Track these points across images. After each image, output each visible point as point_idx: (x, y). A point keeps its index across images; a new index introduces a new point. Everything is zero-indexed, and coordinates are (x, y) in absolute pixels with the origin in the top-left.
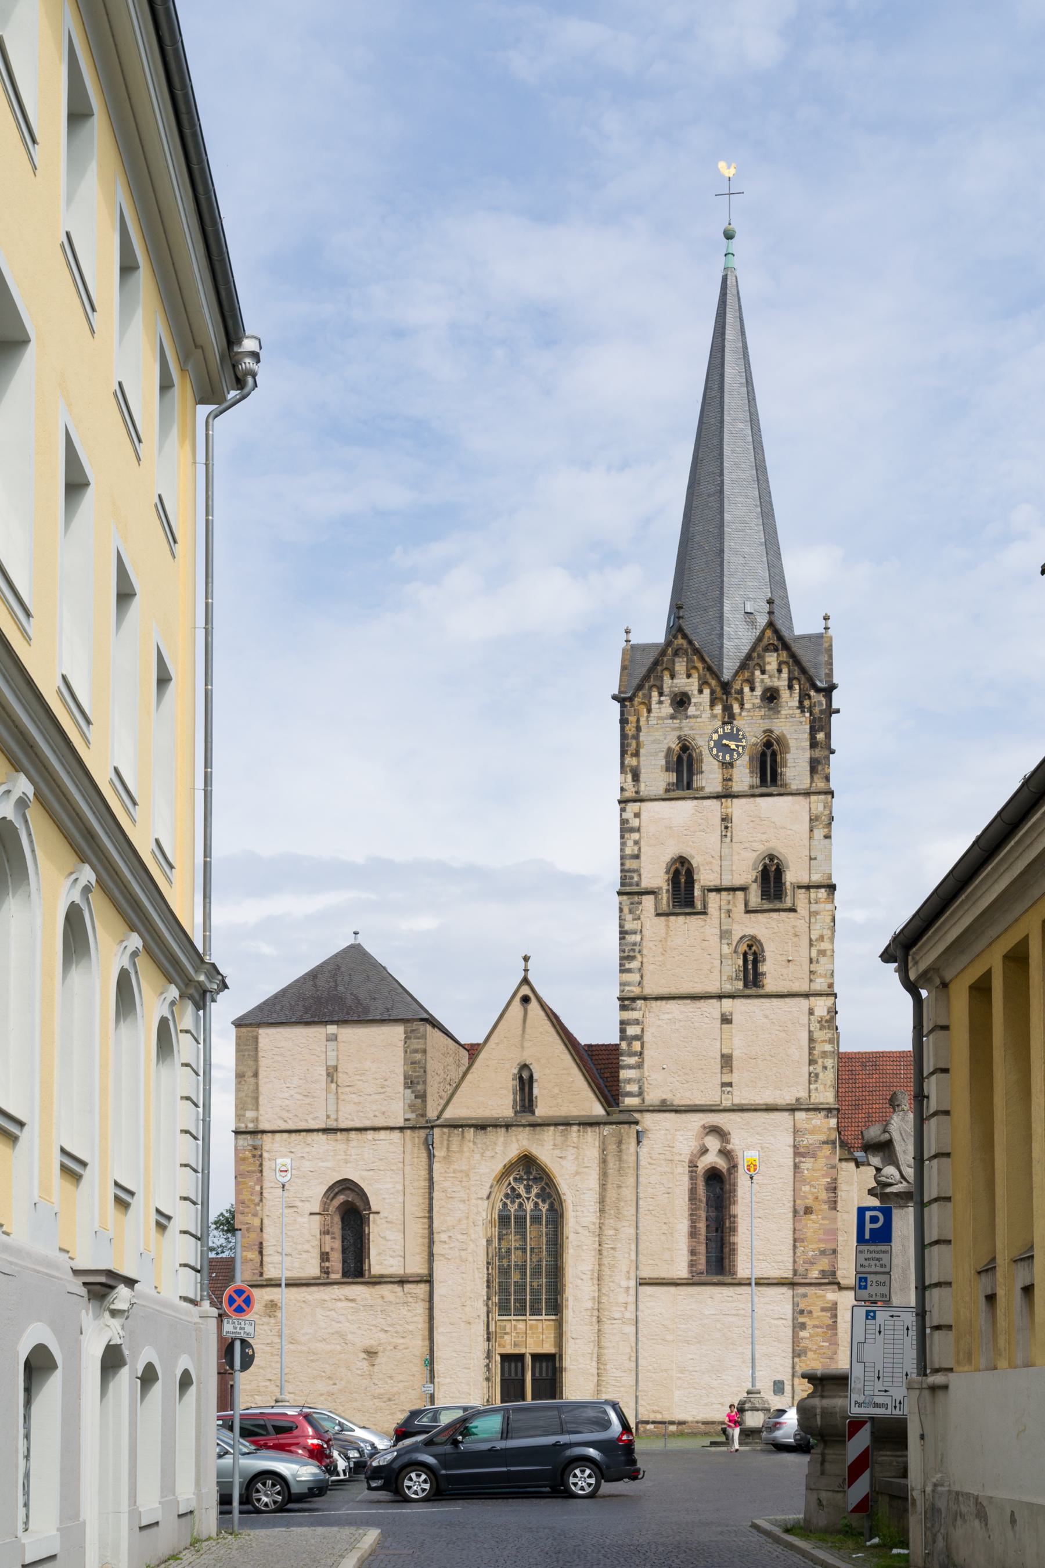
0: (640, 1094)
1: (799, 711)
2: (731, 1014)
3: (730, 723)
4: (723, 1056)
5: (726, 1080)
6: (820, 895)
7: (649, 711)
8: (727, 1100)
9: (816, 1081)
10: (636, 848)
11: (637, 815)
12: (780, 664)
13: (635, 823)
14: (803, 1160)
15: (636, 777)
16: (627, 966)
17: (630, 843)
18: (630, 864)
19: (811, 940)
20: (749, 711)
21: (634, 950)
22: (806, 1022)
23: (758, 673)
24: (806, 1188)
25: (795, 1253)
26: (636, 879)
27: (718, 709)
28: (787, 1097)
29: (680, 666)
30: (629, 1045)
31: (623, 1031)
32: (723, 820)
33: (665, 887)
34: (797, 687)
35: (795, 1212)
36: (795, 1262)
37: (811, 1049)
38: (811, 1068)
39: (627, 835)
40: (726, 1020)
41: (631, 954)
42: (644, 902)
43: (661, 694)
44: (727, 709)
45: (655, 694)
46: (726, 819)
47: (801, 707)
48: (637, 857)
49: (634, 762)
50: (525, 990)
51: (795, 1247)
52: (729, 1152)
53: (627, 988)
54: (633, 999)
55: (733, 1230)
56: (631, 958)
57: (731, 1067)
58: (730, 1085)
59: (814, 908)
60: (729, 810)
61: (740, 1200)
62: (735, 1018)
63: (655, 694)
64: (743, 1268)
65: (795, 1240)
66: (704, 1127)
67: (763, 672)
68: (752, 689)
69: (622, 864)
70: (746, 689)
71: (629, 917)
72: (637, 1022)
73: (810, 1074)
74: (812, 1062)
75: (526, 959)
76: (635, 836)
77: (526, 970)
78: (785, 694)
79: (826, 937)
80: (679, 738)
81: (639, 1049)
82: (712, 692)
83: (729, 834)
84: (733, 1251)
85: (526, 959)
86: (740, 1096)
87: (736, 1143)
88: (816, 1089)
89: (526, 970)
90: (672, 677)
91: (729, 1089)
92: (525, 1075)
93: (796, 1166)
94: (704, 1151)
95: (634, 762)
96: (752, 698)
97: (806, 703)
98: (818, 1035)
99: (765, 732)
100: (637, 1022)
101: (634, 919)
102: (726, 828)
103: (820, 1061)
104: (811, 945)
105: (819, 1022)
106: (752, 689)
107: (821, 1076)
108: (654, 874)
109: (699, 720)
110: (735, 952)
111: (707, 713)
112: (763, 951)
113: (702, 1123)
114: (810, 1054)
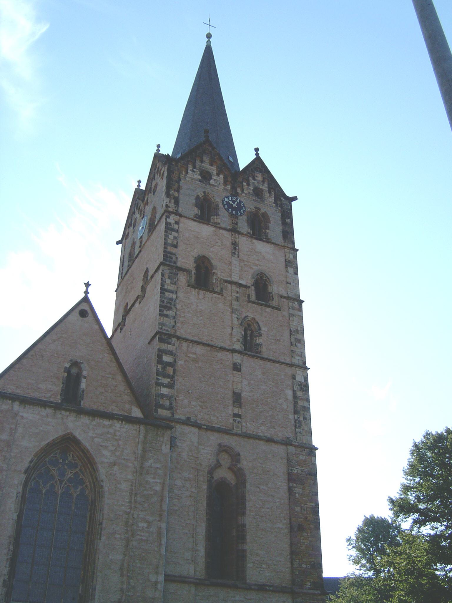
0: (170, 408)
1: (274, 205)
2: (240, 365)
3: (236, 196)
4: (234, 394)
5: (236, 411)
6: (294, 305)
7: (187, 173)
8: (237, 427)
9: (300, 427)
10: (175, 242)
11: (177, 223)
12: (264, 178)
13: (176, 227)
14: (295, 485)
15: (177, 202)
16: (165, 312)
17: (171, 237)
18: (170, 249)
19: (290, 330)
20: (246, 194)
21: (171, 303)
22: (290, 383)
23: (251, 178)
24: (298, 509)
25: (292, 564)
26: (174, 259)
27: (228, 187)
28: (280, 435)
29: (206, 159)
30: (164, 368)
31: (160, 357)
32: (233, 244)
33: (194, 271)
34: (273, 193)
35: (291, 528)
36: (292, 572)
37: (296, 403)
38: (296, 416)
39: (169, 232)
40: (237, 368)
41: (169, 305)
42: (179, 275)
43: (194, 167)
44: (234, 188)
45: (190, 167)
46: (235, 244)
47: (276, 202)
48: (176, 246)
49: (176, 194)
50: (84, 306)
51: (292, 559)
52: (240, 469)
53: (164, 328)
54: (170, 336)
55: (242, 537)
56: (169, 309)
57: (240, 403)
58: (239, 416)
59: (292, 311)
60: (237, 240)
61: (247, 513)
62: (244, 369)
63: (190, 167)
64: (254, 574)
65: (292, 553)
66: (220, 445)
67: (254, 179)
68: (248, 185)
69: (165, 248)
70: (245, 184)
71: (168, 281)
72: (170, 353)
73: (295, 420)
74: (296, 412)
75: (87, 285)
76: (175, 234)
77: (86, 292)
78: (267, 194)
79: (300, 332)
80: (204, 192)
81: (171, 373)
82: (225, 178)
83: (237, 253)
84: (242, 556)
85: (87, 285)
86: (249, 427)
87: (244, 464)
88: (300, 433)
89: (86, 292)
90: (202, 162)
91: (239, 419)
92: (74, 371)
93: (290, 490)
94: (218, 465)
95: (176, 194)
96: (249, 189)
97: (279, 203)
98: (299, 393)
99: (256, 208)
100: (170, 353)
101: (172, 283)
102: (235, 249)
103: (302, 412)
104: (291, 334)
105: (299, 385)
106: (248, 185)
107: (303, 423)
108: (186, 259)
109: (216, 188)
110: (241, 324)
111: (222, 187)
112: (260, 329)
113: (219, 441)
114: (295, 406)
